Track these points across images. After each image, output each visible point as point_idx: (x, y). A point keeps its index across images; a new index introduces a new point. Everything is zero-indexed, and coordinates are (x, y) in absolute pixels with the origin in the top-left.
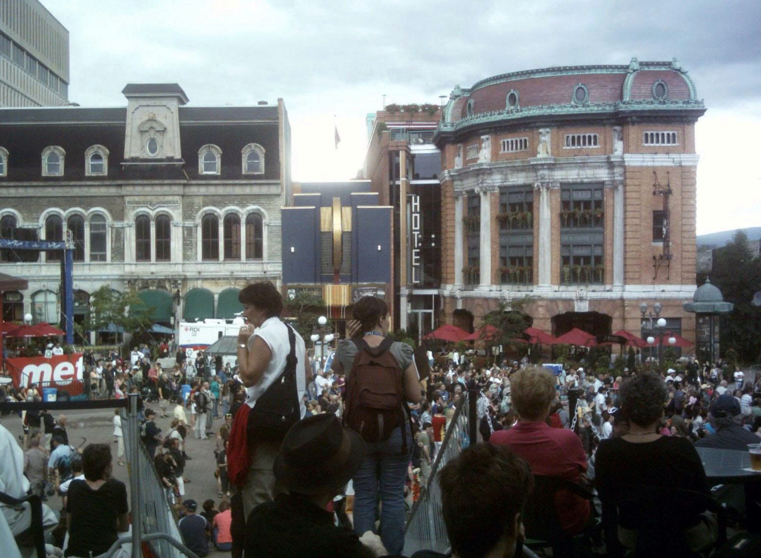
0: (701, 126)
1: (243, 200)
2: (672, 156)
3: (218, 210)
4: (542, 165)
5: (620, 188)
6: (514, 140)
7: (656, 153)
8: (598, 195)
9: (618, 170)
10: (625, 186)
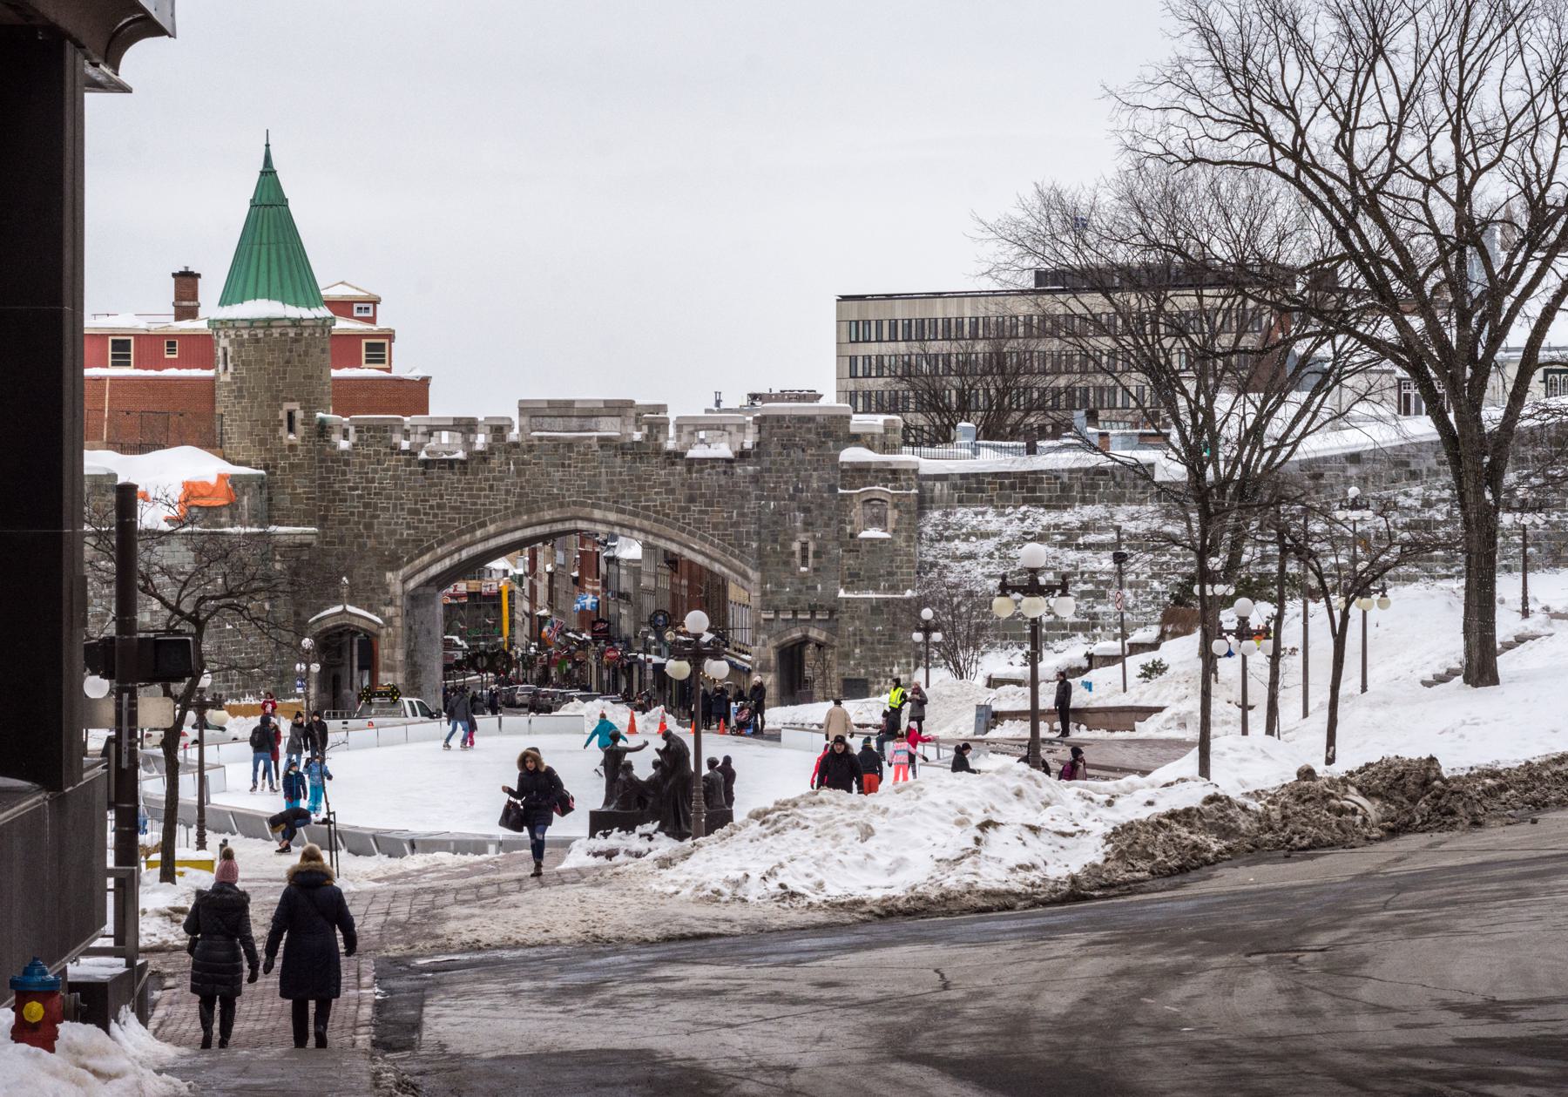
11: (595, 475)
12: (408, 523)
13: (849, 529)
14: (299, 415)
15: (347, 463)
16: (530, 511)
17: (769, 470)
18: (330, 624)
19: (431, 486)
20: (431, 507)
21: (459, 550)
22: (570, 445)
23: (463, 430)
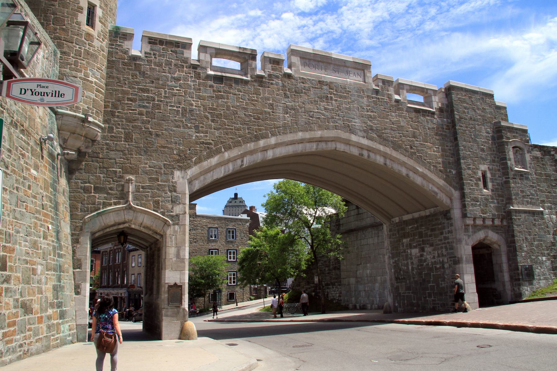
11: (349, 109)
12: (197, 127)
15: (138, 67)
16: (305, 130)
19: (218, 97)
20: (219, 116)
22: (330, 85)
23: (247, 57)
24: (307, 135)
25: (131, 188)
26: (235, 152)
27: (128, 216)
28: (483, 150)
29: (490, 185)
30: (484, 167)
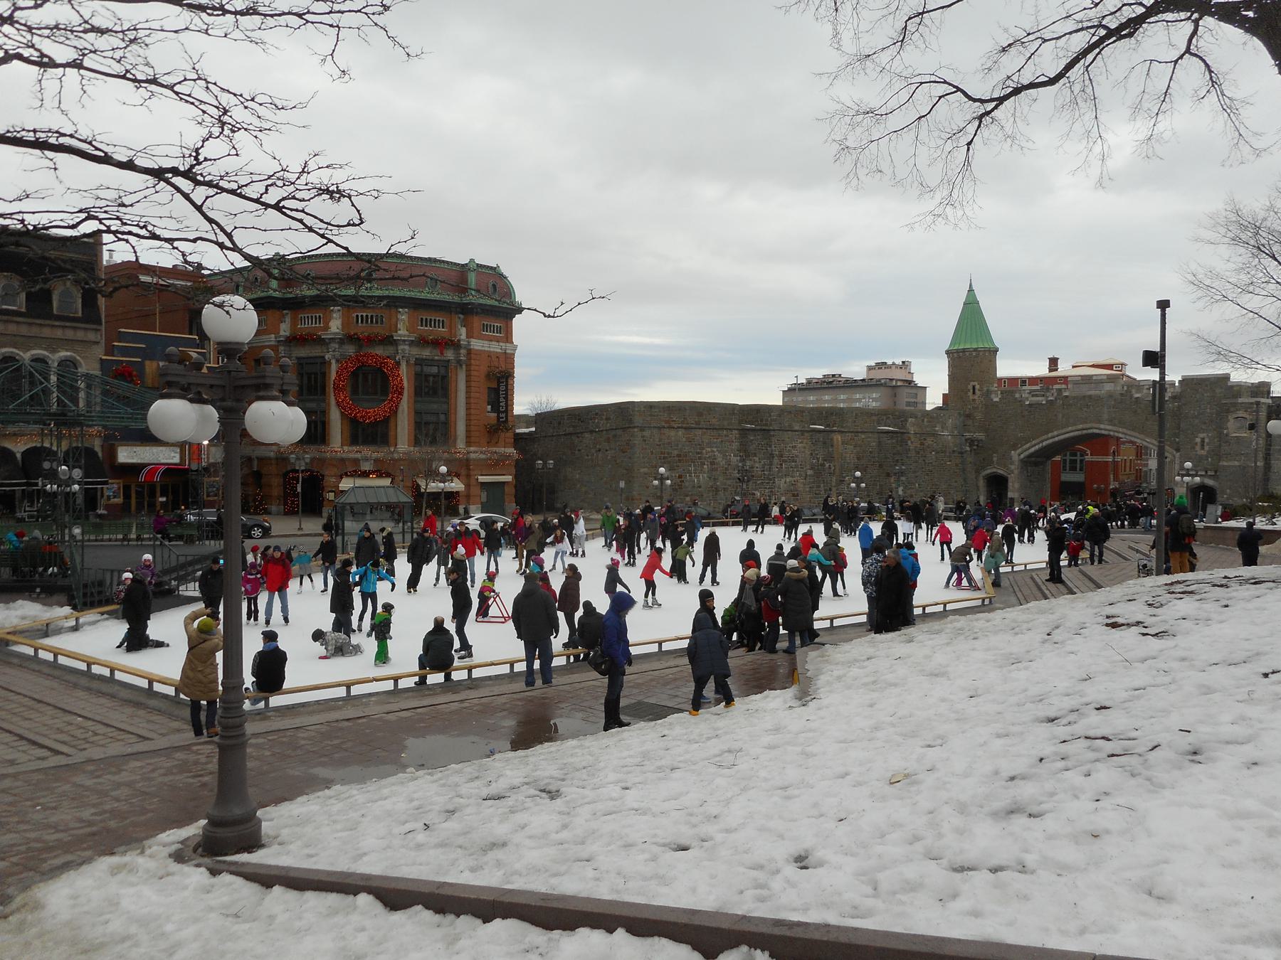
0: (517, 321)
1: (53, 345)
2: (501, 344)
3: (21, 354)
4: (404, 341)
5: (464, 366)
6: (369, 315)
7: (491, 341)
8: (443, 371)
9: (463, 351)
10: (468, 365)
13: (1225, 431)
14: (977, 387)
15: (997, 406)
17: (1184, 404)
18: (989, 471)
21: (1042, 441)
22: (1090, 397)
24: (1074, 428)
25: (995, 459)
26: (1037, 441)
27: (995, 470)
28: (1205, 423)
29: (1207, 448)
30: (1202, 435)
